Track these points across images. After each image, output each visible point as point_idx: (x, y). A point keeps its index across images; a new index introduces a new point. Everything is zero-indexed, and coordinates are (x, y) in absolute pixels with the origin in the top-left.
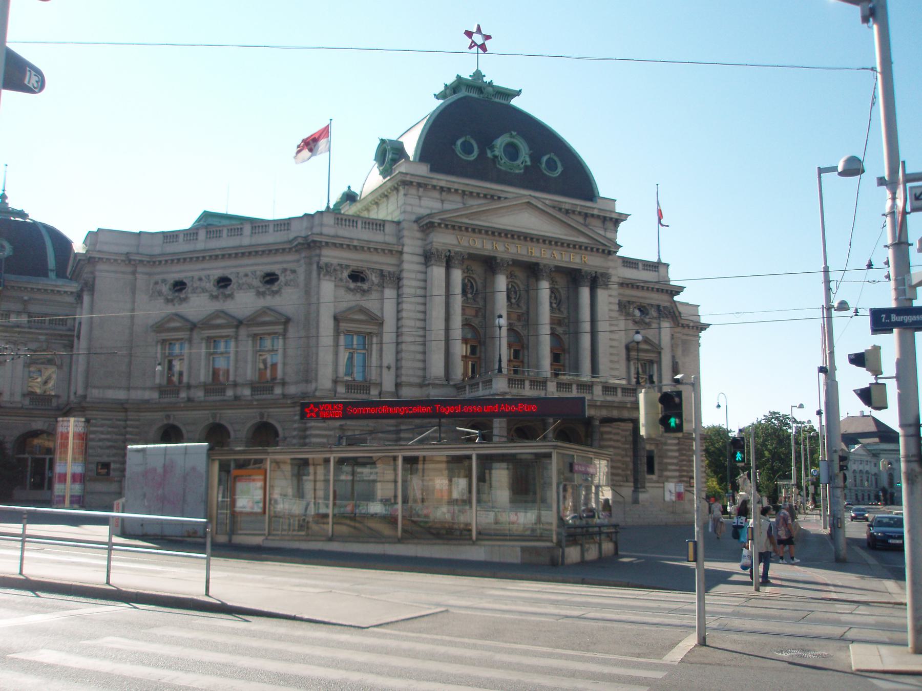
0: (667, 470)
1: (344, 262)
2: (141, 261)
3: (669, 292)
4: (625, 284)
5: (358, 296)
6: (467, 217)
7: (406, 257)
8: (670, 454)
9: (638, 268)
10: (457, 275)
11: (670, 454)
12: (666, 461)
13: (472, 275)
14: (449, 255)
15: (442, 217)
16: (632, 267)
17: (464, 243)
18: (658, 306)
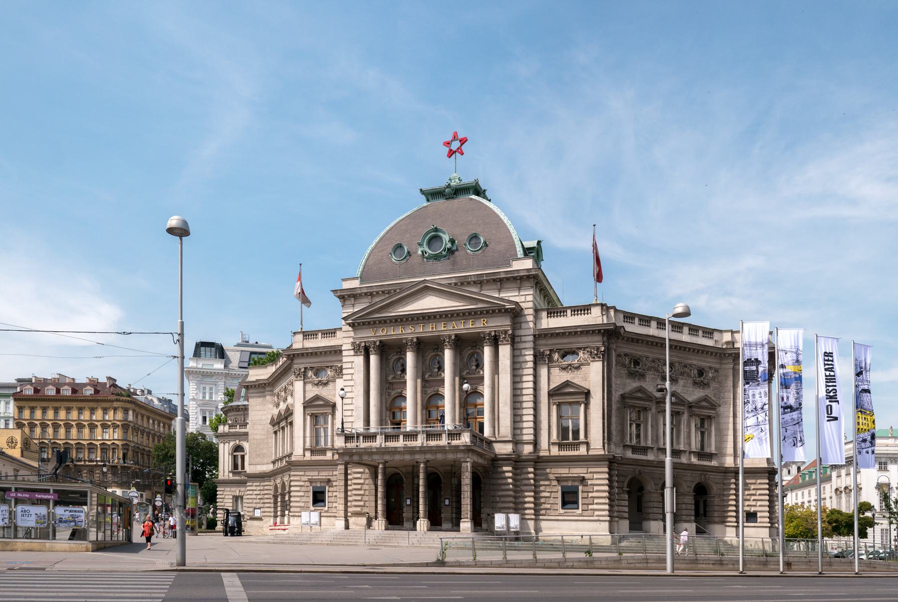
0: (593, 504)
1: (308, 366)
2: (265, 384)
3: (597, 332)
4: (541, 336)
5: (321, 387)
6: (377, 312)
7: (344, 353)
8: (596, 488)
9: (566, 315)
10: (373, 359)
11: (596, 488)
12: (590, 495)
13: (402, 356)
14: (365, 345)
15: (352, 318)
16: (560, 316)
17: (380, 333)
18: (587, 347)
